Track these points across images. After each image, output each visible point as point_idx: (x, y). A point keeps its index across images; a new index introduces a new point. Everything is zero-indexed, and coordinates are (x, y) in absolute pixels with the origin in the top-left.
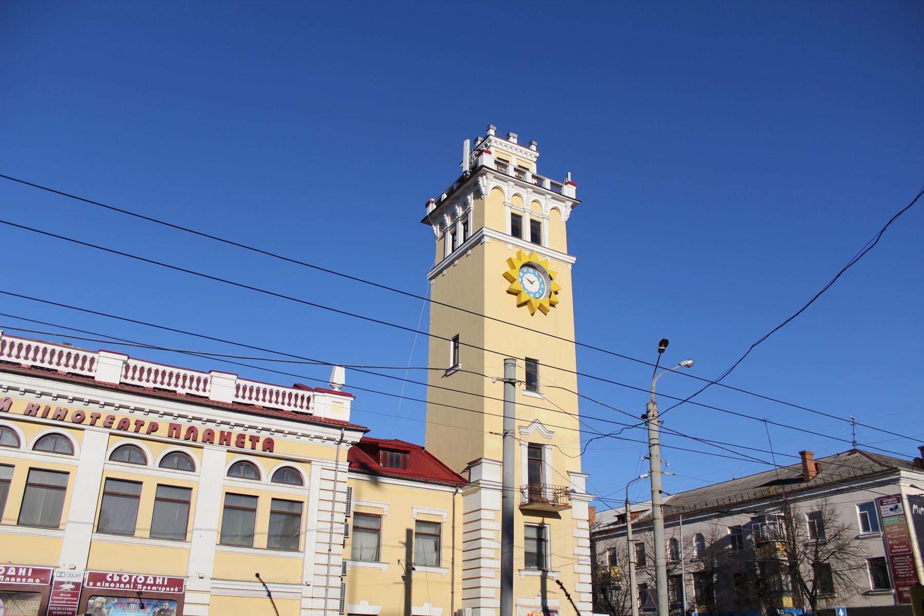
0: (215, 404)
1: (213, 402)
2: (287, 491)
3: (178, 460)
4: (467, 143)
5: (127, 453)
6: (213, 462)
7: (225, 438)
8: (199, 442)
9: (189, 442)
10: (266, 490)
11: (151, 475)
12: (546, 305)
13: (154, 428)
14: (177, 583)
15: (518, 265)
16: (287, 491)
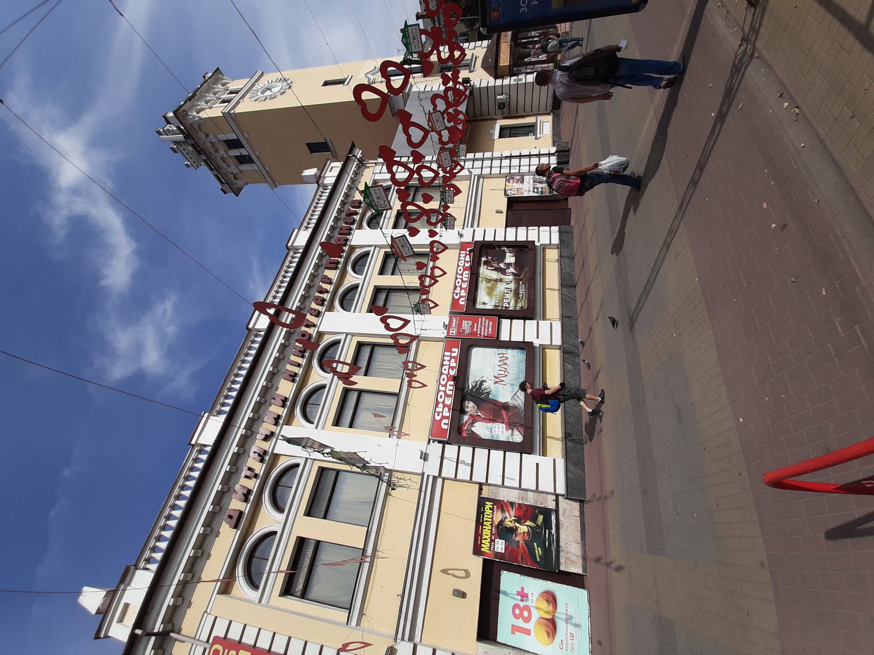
14: (463, 246)
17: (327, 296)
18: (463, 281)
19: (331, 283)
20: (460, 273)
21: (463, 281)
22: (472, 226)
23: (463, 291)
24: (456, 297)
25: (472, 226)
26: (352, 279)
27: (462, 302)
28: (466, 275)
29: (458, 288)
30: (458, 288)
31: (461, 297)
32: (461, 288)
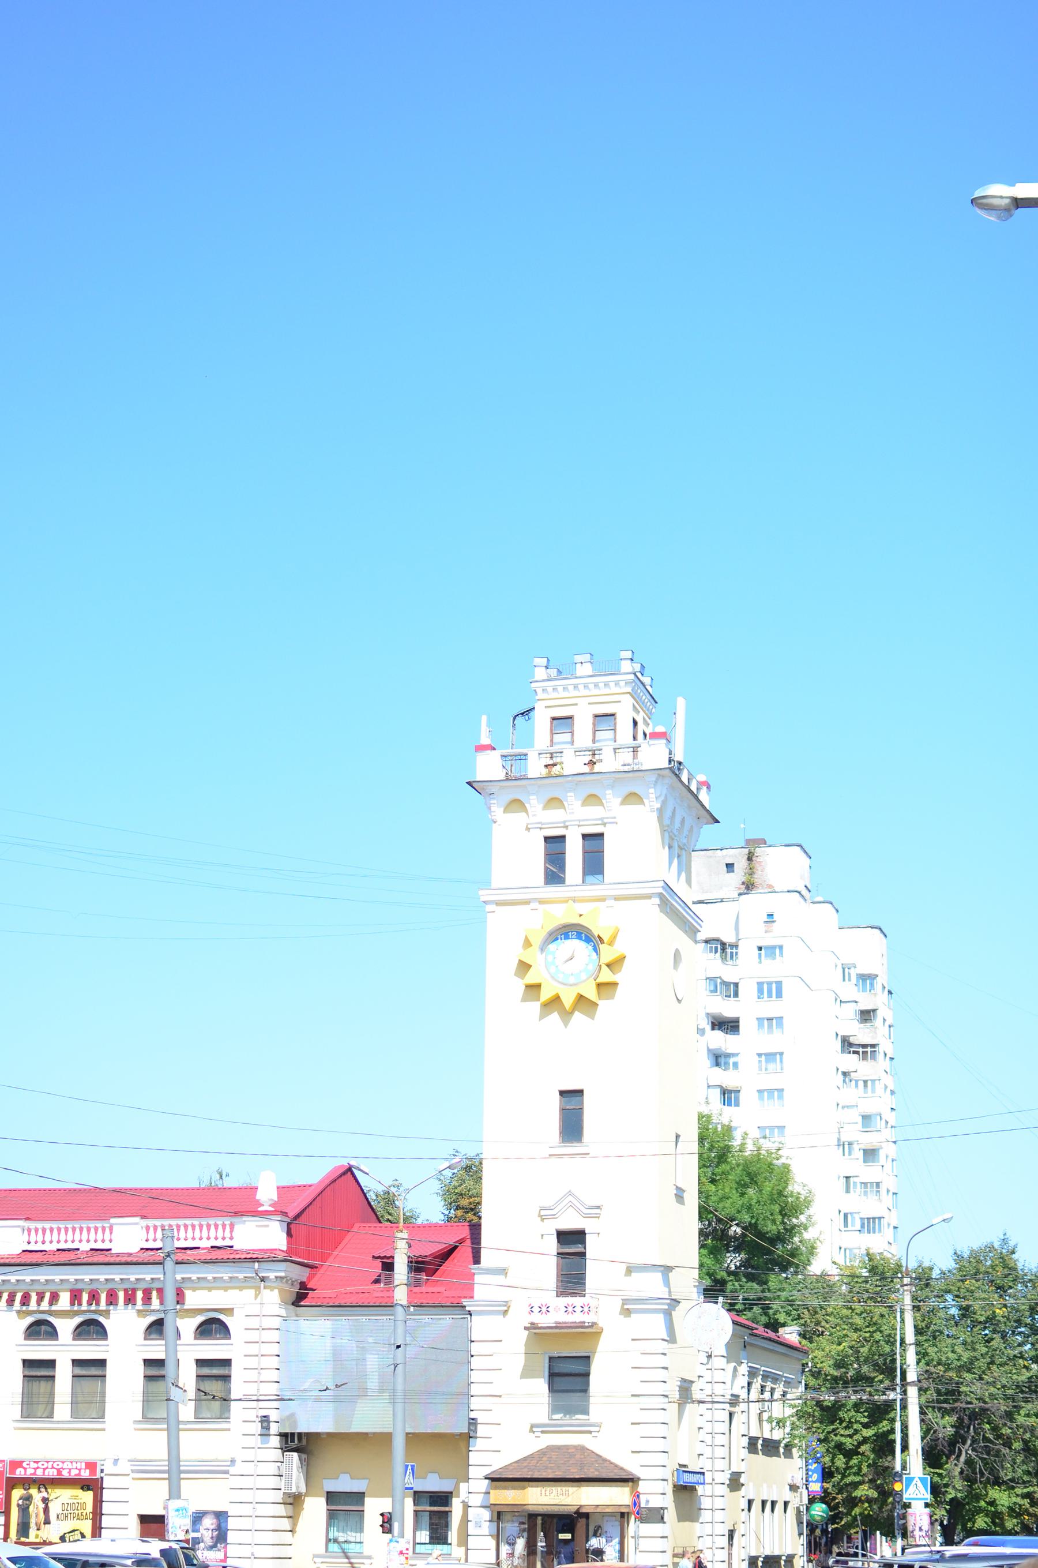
0: (124, 1259)
1: (118, 1255)
2: (212, 1349)
3: (91, 1328)
4: (484, 718)
5: (41, 1329)
6: (125, 1325)
7: (130, 1299)
8: (103, 1306)
9: (93, 1307)
10: (189, 1351)
11: (65, 1350)
12: (591, 993)
13: (54, 1298)
15: (537, 940)
16: (212, 1349)
17: (33, 1305)
18: (44, 1469)
19: (51, 1304)
20: (55, 1465)
21: (44, 1469)
22: (133, 1471)
23: (33, 1471)
24: (24, 1465)
25: (133, 1471)
26: (65, 1327)
27: (20, 1473)
28: (51, 1473)
29: (35, 1465)
30: (35, 1465)
31: (25, 1469)
32: (35, 1469)
